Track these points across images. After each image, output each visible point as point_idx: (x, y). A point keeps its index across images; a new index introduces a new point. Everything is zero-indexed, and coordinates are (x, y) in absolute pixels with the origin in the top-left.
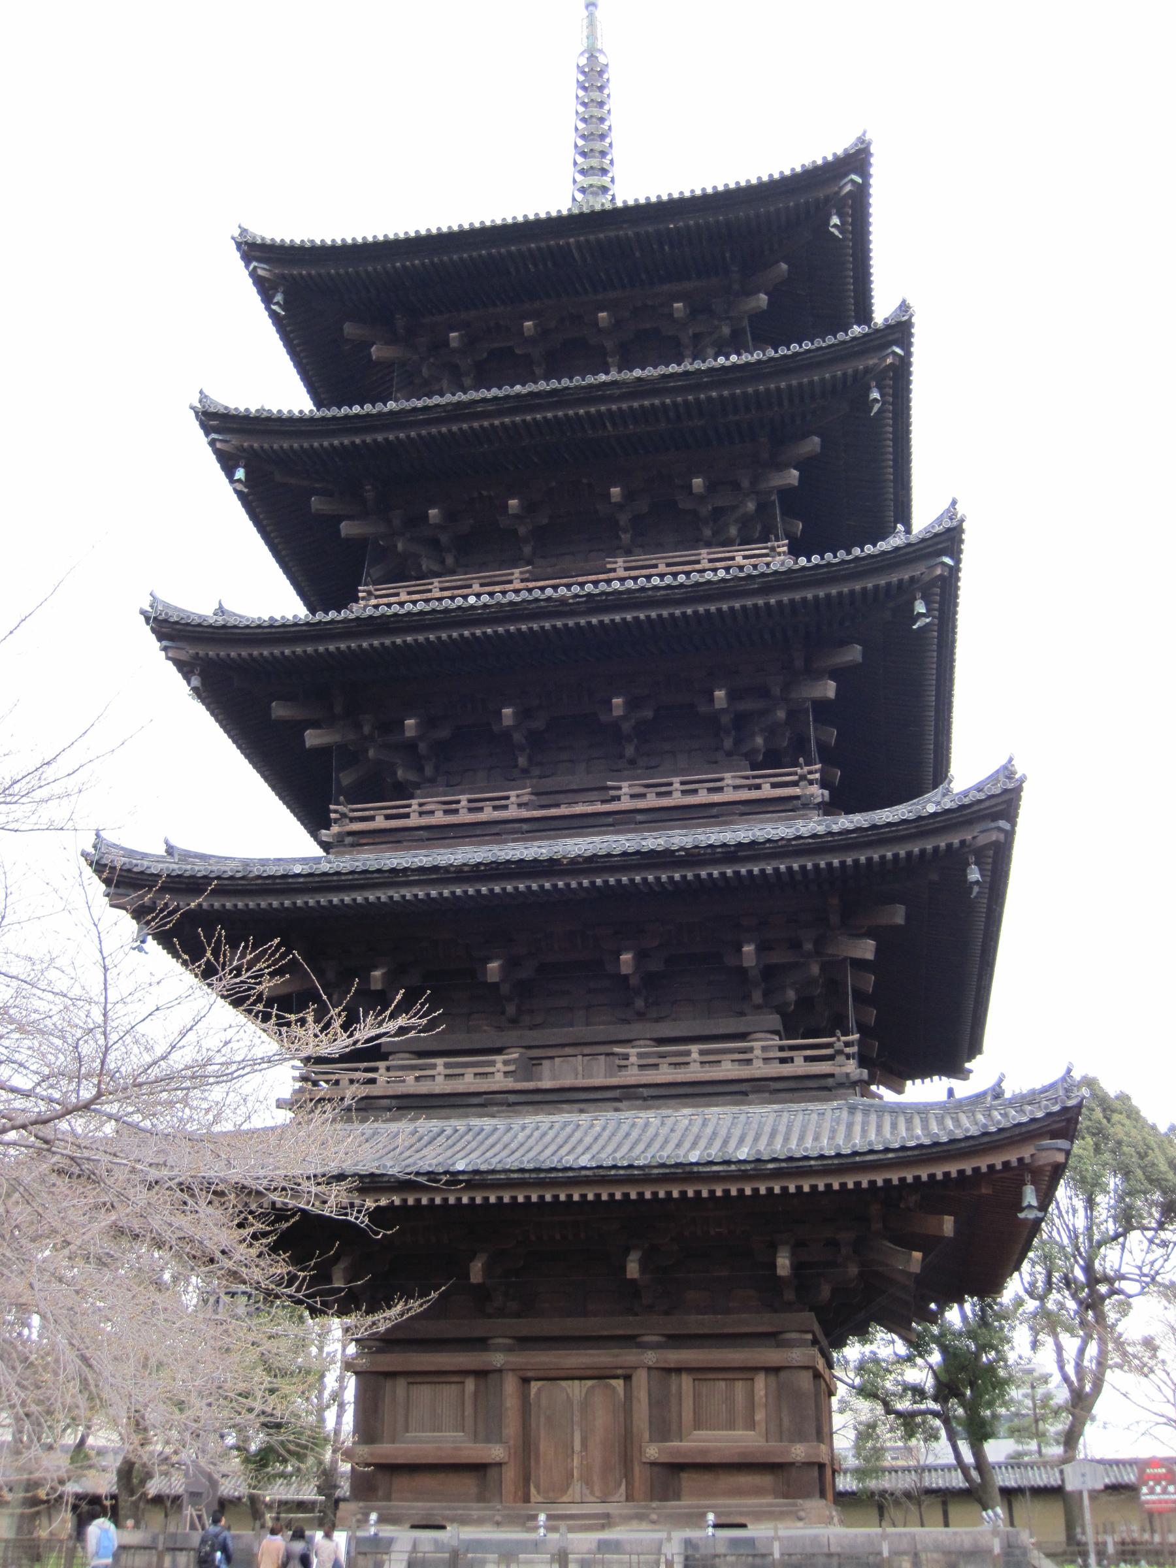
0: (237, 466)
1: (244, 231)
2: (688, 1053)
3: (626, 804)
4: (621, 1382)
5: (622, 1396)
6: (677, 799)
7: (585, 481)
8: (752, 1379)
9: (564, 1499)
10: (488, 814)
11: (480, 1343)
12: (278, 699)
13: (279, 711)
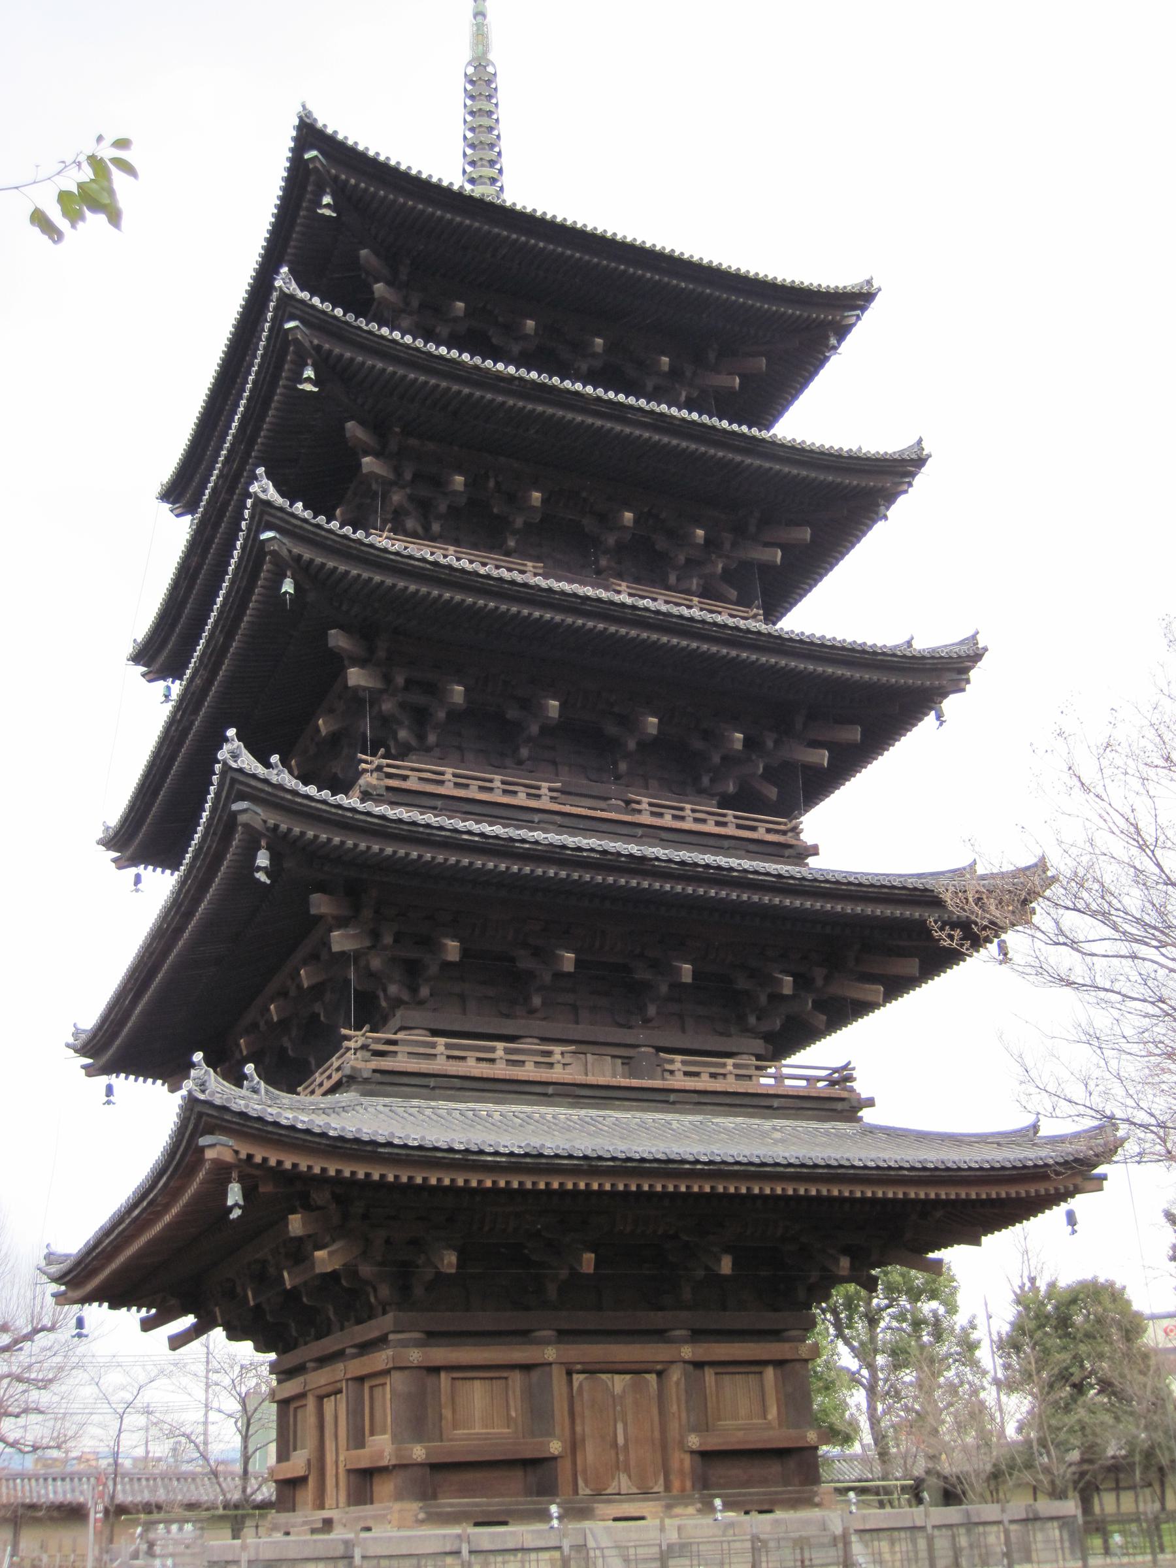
1: (309, 114)
2: (724, 1065)
4: (654, 1376)
5: (655, 1386)
6: (688, 825)
7: (584, 494)
8: (761, 1373)
9: (609, 1491)
10: (521, 799)
11: (522, 1335)
12: (341, 627)
13: (337, 639)
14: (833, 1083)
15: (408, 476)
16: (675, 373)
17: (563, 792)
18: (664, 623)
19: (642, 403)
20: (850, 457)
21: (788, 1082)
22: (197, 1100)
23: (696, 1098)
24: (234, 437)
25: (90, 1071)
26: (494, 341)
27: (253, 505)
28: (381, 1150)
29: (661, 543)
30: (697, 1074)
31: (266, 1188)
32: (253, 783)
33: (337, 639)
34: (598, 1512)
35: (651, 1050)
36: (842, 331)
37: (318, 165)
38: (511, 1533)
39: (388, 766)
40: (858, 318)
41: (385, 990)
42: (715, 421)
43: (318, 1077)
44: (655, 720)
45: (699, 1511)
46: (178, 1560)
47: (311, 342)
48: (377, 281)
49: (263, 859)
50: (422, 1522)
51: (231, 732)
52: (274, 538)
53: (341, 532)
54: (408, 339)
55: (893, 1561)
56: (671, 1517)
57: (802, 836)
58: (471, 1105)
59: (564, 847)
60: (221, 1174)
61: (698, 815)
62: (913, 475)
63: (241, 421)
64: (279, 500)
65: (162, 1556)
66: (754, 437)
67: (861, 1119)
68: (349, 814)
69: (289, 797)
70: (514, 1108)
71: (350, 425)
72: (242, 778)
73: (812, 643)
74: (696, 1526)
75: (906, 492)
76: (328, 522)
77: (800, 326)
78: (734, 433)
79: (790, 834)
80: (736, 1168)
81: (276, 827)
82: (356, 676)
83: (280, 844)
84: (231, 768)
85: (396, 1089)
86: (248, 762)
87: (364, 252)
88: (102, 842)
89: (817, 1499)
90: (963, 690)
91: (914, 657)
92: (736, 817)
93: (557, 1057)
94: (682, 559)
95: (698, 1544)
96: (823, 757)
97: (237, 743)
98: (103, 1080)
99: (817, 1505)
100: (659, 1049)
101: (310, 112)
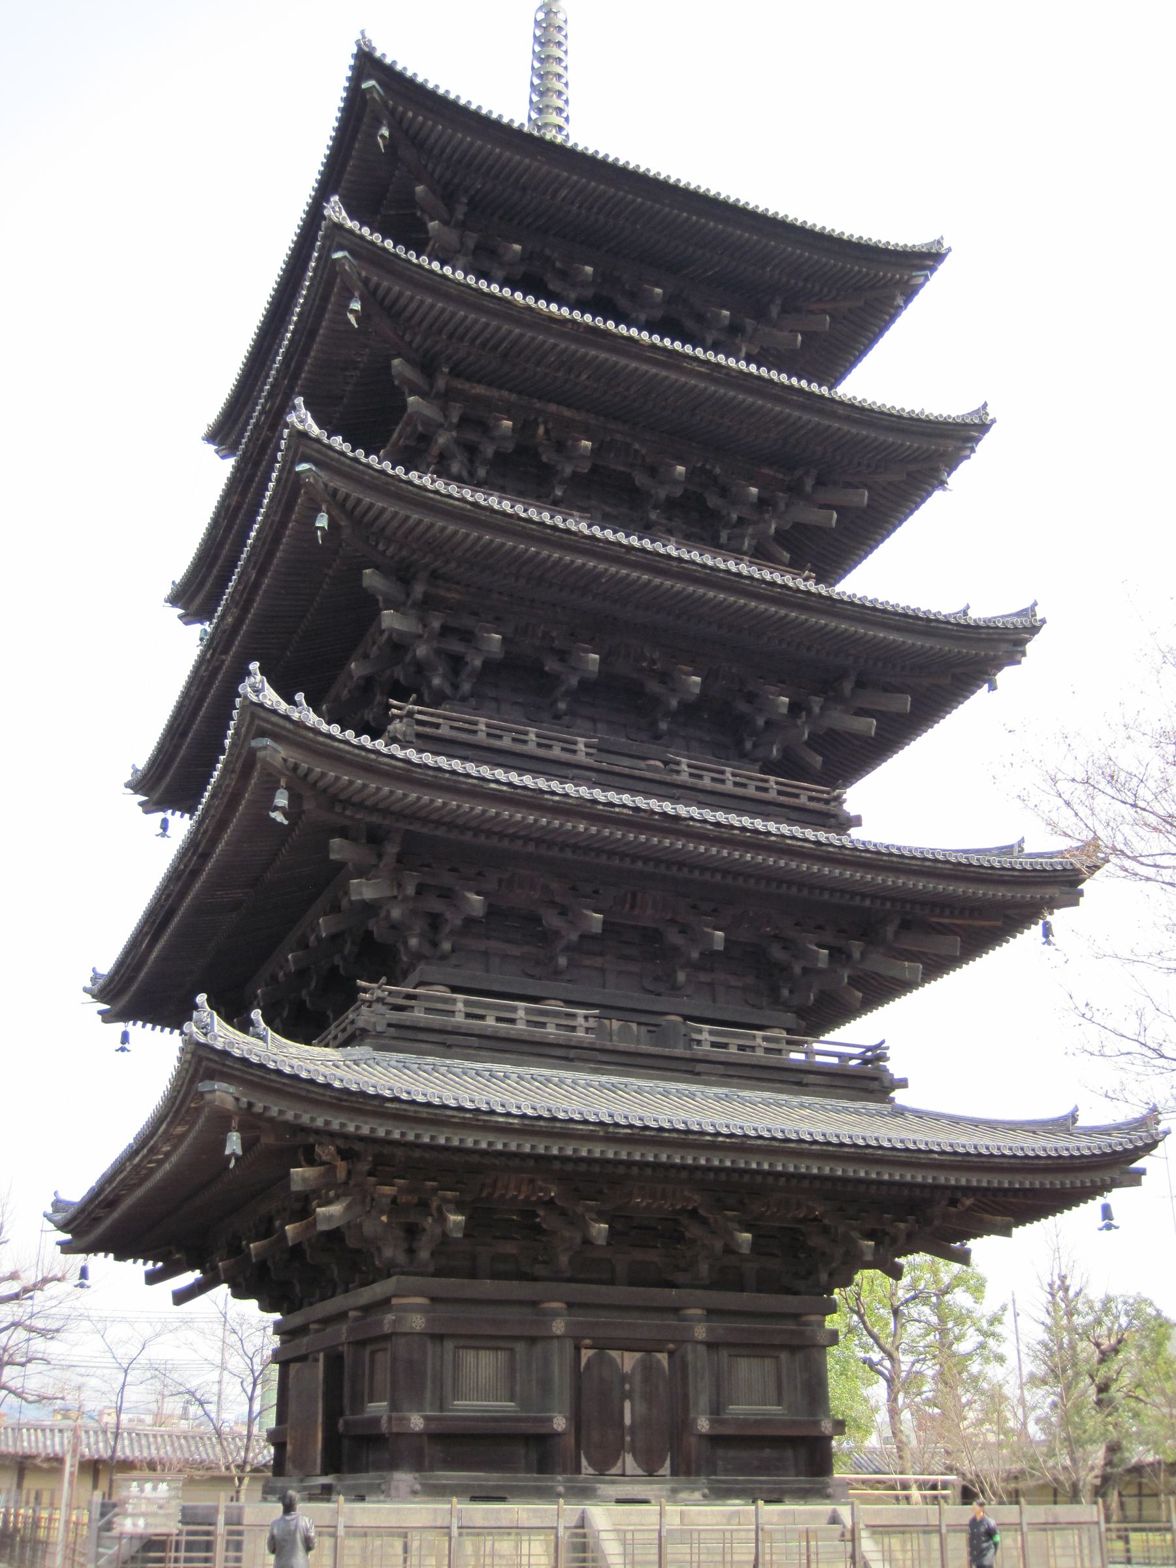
0: (350, 298)
3: (684, 778)
4: (666, 1355)
6: (729, 787)
10: (556, 752)
12: (377, 567)
13: (370, 578)
14: (866, 1062)
15: (455, 420)
16: (734, 329)
17: (600, 750)
18: (711, 578)
19: (699, 352)
20: (912, 419)
21: (819, 1058)
22: (198, 1044)
23: (721, 1069)
24: (278, 371)
25: (107, 1017)
26: (551, 287)
27: (290, 435)
28: (389, 1105)
29: (713, 501)
30: (725, 1046)
31: (267, 1140)
32: (275, 719)
33: (370, 578)
34: (599, 1492)
35: (679, 1019)
36: (910, 292)
37: (376, 96)
38: (506, 1510)
39: (420, 712)
40: (927, 279)
41: (405, 943)
42: (774, 375)
43: (333, 1030)
44: (698, 679)
45: (704, 1496)
46: (151, 1520)
47: (359, 274)
48: (432, 219)
49: (282, 800)
50: (415, 1493)
51: (254, 666)
52: (310, 470)
53: (378, 467)
54: (460, 275)
55: (904, 1560)
56: (675, 1502)
57: (846, 807)
58: (488, 1065)
59: (595, 802)
60: (221, 1122)
61: (738, 779)
62: (977, 440)
63: (285, 355)
64: (315, 430)
65: (134, 1515)
66: (812, 394)
67: (893, 1099)
68: (373, 756)
69: (311, 735)
70: (534, 1070)
71: (396, 362)
72: (263, 714)
73: (863, 606)
74: (700, 1512)
75: (968, 457)
76: (367, 456)
77: (865, 284)
78: (791, 388)
79: (833, 804)
80: (760, 1142)
81: (296, 767)
82: (389, 619)
83: (300, 784)
84: (252, 703)
85: (410, 1044)
86: (270, 697)
87: (420, 189)
88: (127, 785)
89: (830, 1490)
90: (1019, 663)
91: (968, 626)
92: (777, 783)
93: (580, 1021)
94: (734, 516)
95: (699, 1531)
96: (870, 725)
97: (259, 677)
98: (120, 1027)
99: (828, 1497)
100: (687, 1018)
101: (370, 41)
